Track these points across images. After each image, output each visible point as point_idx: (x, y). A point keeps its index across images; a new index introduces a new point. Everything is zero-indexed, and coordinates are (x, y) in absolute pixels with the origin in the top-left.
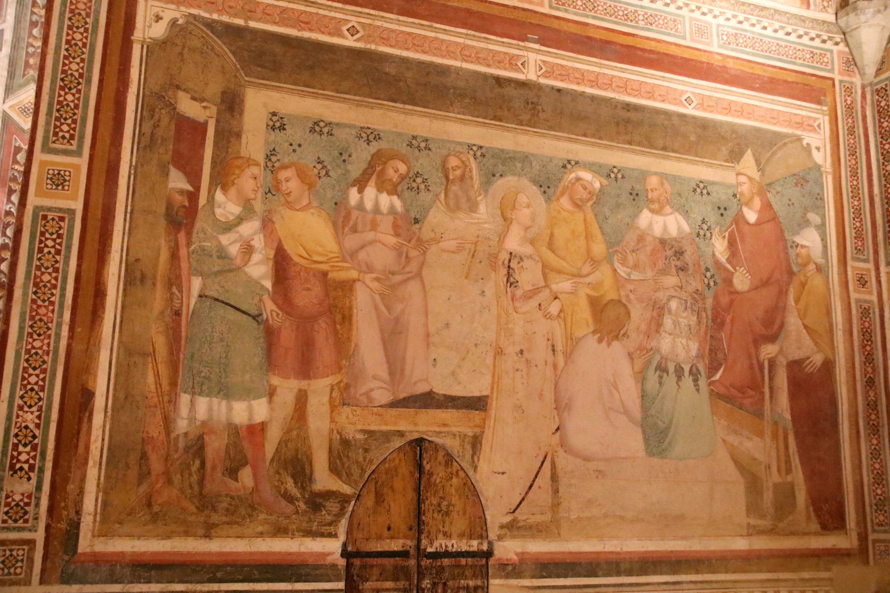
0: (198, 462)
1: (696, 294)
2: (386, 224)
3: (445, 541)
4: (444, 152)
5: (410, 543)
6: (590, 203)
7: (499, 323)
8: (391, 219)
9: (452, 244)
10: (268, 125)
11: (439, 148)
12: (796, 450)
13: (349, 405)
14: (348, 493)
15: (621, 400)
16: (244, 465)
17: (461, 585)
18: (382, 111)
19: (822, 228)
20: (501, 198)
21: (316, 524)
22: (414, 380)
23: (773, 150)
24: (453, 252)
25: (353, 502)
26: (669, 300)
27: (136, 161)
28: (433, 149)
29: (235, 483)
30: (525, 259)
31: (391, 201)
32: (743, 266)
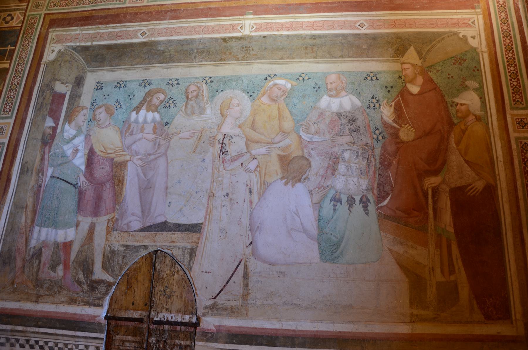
0: (37, 262)
1: (367, 146)
2: (149, 128)
3: (166, 314)
4: (188, 84)
5: (145, 314)
6: (284, 97)
7: (213, 176)
8: (153, 124)
9: (187, 134)
10: (94, 89)
11: (185, 83)
12: (459, 255)
13: (117, 230)
14: (111, 281)
15: (301, 223)
16: (59, 264)
17: (176, 344)
18: (154, 70)
19: (480, 91)
20: (221, 103)
21: (92, 298)
22: (156, 215)
23: (432, 44)
24: (188, 139)
25: (114, 287)
26: (343, 152)
27: (33, 118)
28: (181, 84)
29: (54, 273)
30: (234, 137)
31: (153, 115)
32: (408, 123)
